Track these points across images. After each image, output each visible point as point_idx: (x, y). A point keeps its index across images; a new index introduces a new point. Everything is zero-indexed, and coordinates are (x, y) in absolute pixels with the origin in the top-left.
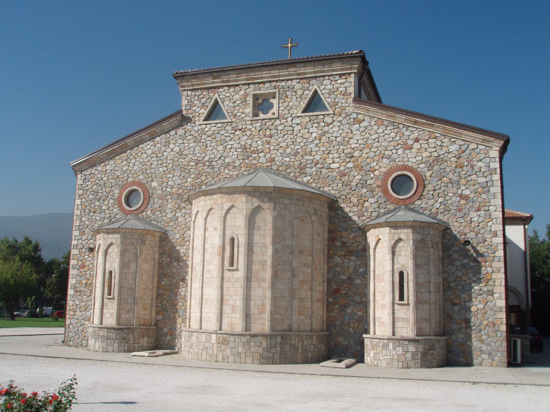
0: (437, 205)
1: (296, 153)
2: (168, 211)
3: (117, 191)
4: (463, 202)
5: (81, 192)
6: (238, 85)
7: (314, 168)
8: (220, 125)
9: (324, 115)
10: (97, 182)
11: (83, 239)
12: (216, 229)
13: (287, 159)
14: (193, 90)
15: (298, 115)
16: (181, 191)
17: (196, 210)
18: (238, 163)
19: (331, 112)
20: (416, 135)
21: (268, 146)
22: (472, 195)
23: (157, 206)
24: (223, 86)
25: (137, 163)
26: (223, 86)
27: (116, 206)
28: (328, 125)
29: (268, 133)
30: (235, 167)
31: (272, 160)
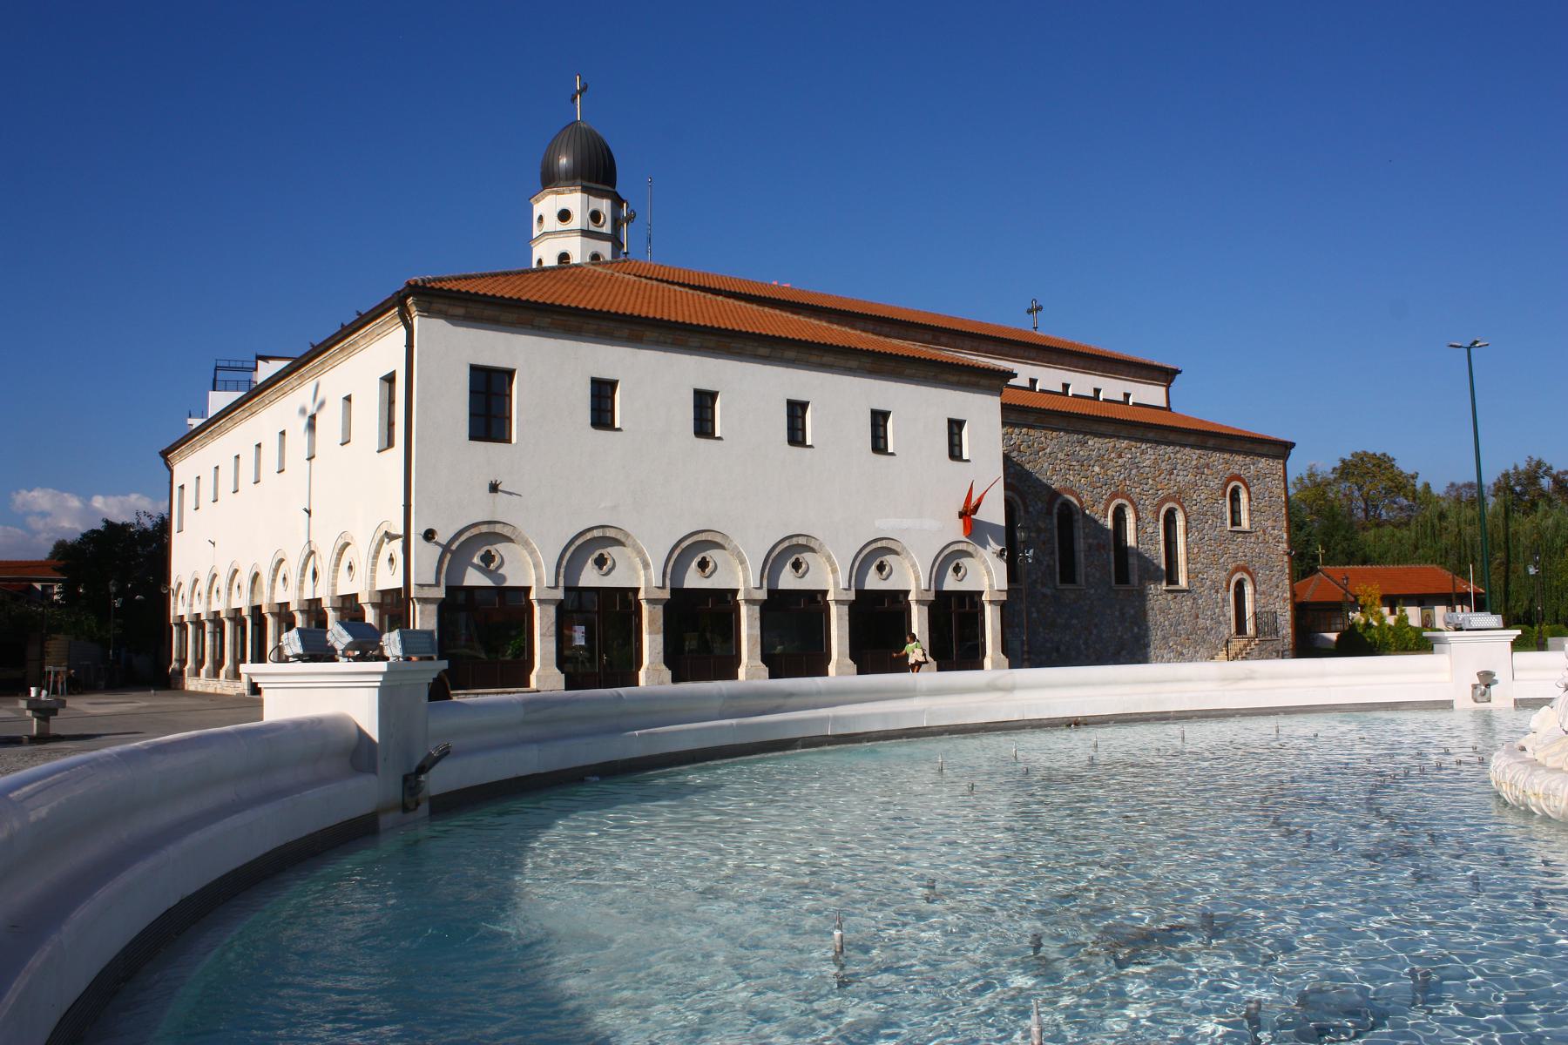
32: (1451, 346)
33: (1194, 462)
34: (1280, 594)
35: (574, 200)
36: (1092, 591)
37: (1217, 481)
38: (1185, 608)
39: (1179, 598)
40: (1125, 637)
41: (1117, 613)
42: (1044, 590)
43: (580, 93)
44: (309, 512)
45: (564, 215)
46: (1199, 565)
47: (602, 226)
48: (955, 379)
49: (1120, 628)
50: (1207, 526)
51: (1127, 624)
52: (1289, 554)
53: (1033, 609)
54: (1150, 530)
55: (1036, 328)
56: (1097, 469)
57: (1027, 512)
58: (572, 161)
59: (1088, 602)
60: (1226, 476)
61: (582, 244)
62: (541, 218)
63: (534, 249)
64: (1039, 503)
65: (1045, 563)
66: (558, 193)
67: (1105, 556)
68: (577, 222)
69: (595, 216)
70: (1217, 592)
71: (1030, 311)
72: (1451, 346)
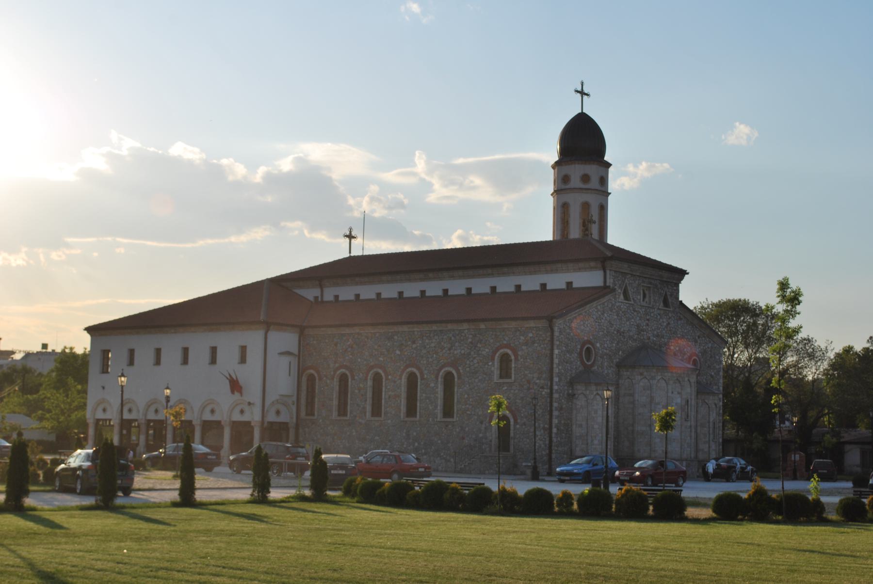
0: (704, 380)
1: (658, 336)
2: (605, 368)
3: (579, 347)
4: (712, 379)
5: (558, 343)
6: (635, 275)
7: (665, 348)
8: (627, 305)
9: (668, 311)
10: (568, 336)
11: (561, 385)
12: (679, 393)
13: (655, 339)
14: (615, 272)
15: (660, 307)
16: (610, 353)
17: (661, 377)
18: (636, 337)
19: (671, 309)
20: (698, 334)
21: (647, 327)
22: (714, 376)
23: (600, 363)
24: (629, 274)
25: (589, 325)
26: (629, 274)
27: (579, 359)
28: (670, 318)
29: (648, 318)
30: (634, 339)
31: (649, 338)
33: (470, 340)
34: (542, 425)
36: (389, 421)
37: (487, 350)
38: (455, 433)
39: (450, 426)
40: (409, 448)
41: (404, 434)
42: (360, 420)
46: (467, 406)
49: (406, 443)
50: (477, 380)
51: (411, 441)
53: (354, 431)
54: (432, 385)
56: (398, 352)
57: (353, 379)
59: (386, 427)
60: (495, 346)
64: (361, 374)
65: (362, 406)
67: (399, 402)
70: (481, 423)
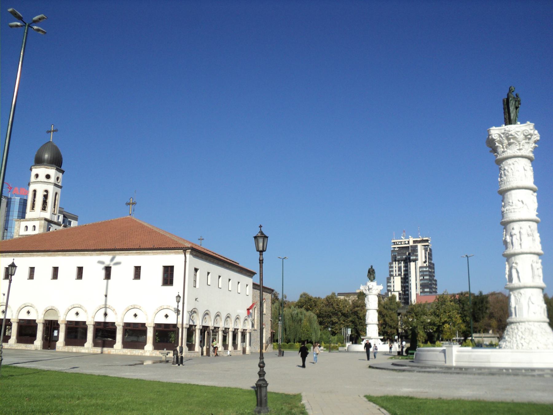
32: (279, 258)
35: (52, 172)
43: (53, 131)
44: (106, 296)
45: (48, 177)
47: (59, 183)
48: (248, 274)
52: (271, 321)
55: (201, 245)
58: (49, 157)
61: (54, 188)
62: (37, 176)
63: (31, 185)
66: (46, 168)
68: (52, 180)
69: (58, 178)
71: (199, 239)
72: (279, 258)
